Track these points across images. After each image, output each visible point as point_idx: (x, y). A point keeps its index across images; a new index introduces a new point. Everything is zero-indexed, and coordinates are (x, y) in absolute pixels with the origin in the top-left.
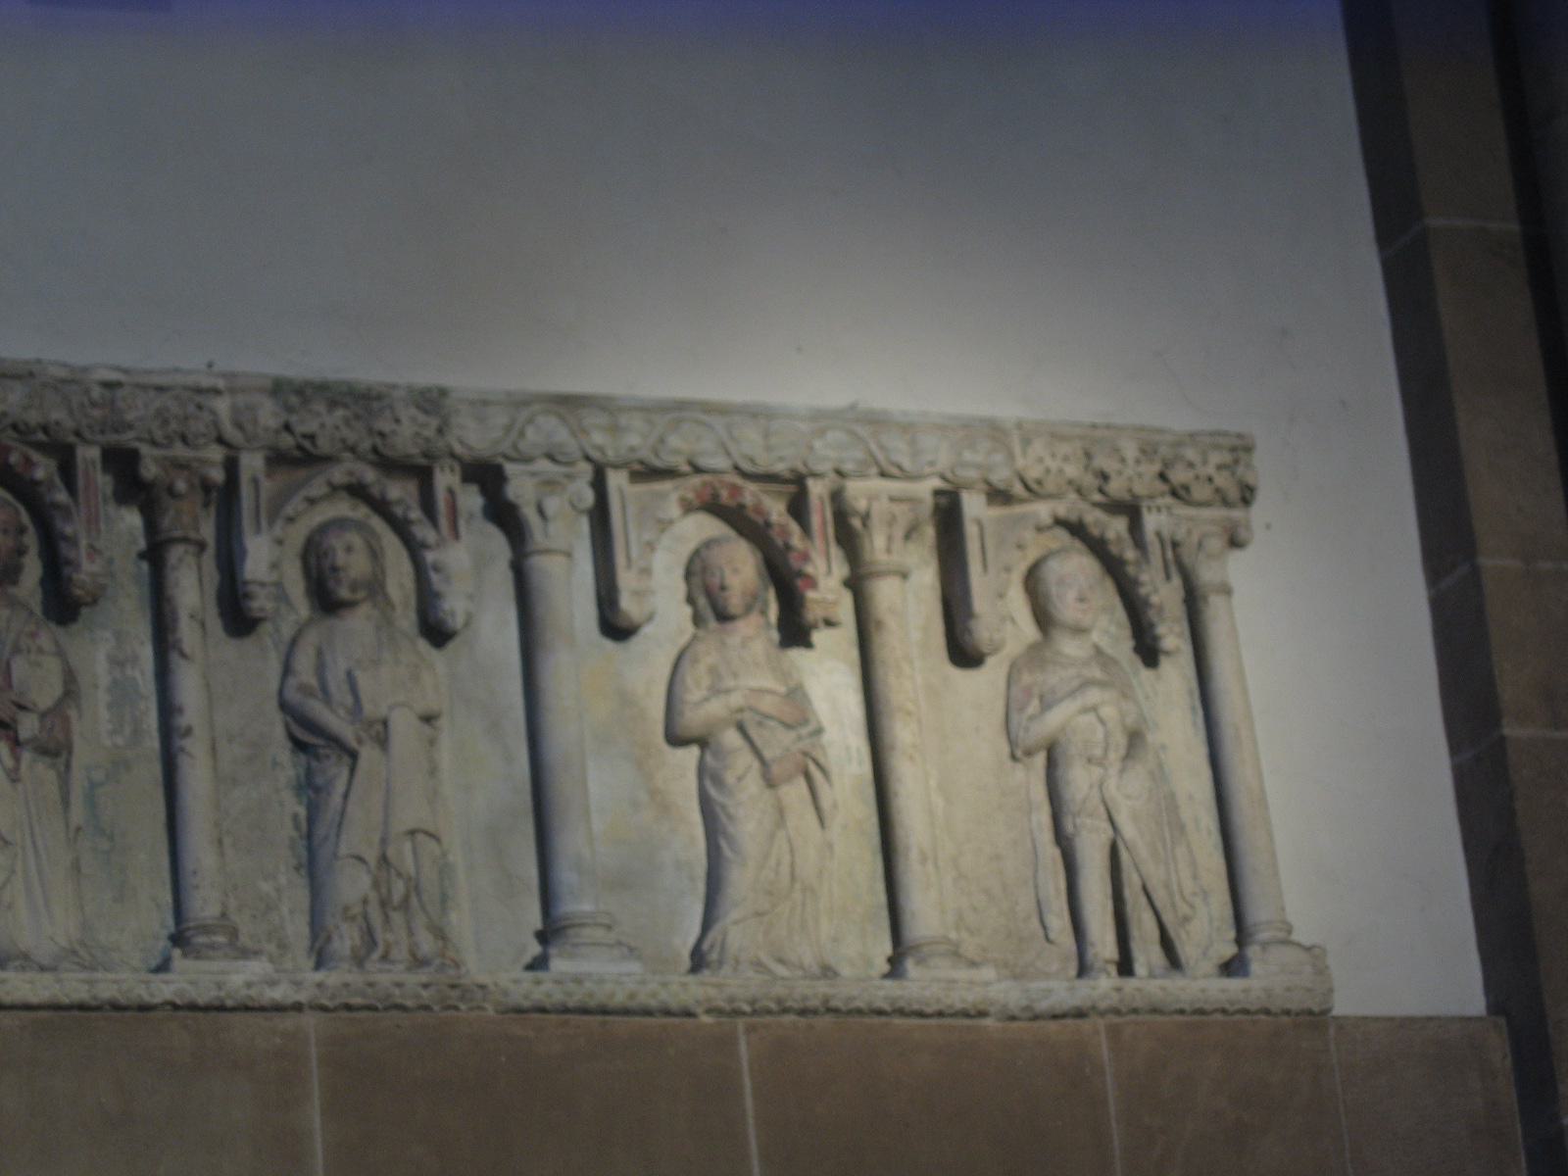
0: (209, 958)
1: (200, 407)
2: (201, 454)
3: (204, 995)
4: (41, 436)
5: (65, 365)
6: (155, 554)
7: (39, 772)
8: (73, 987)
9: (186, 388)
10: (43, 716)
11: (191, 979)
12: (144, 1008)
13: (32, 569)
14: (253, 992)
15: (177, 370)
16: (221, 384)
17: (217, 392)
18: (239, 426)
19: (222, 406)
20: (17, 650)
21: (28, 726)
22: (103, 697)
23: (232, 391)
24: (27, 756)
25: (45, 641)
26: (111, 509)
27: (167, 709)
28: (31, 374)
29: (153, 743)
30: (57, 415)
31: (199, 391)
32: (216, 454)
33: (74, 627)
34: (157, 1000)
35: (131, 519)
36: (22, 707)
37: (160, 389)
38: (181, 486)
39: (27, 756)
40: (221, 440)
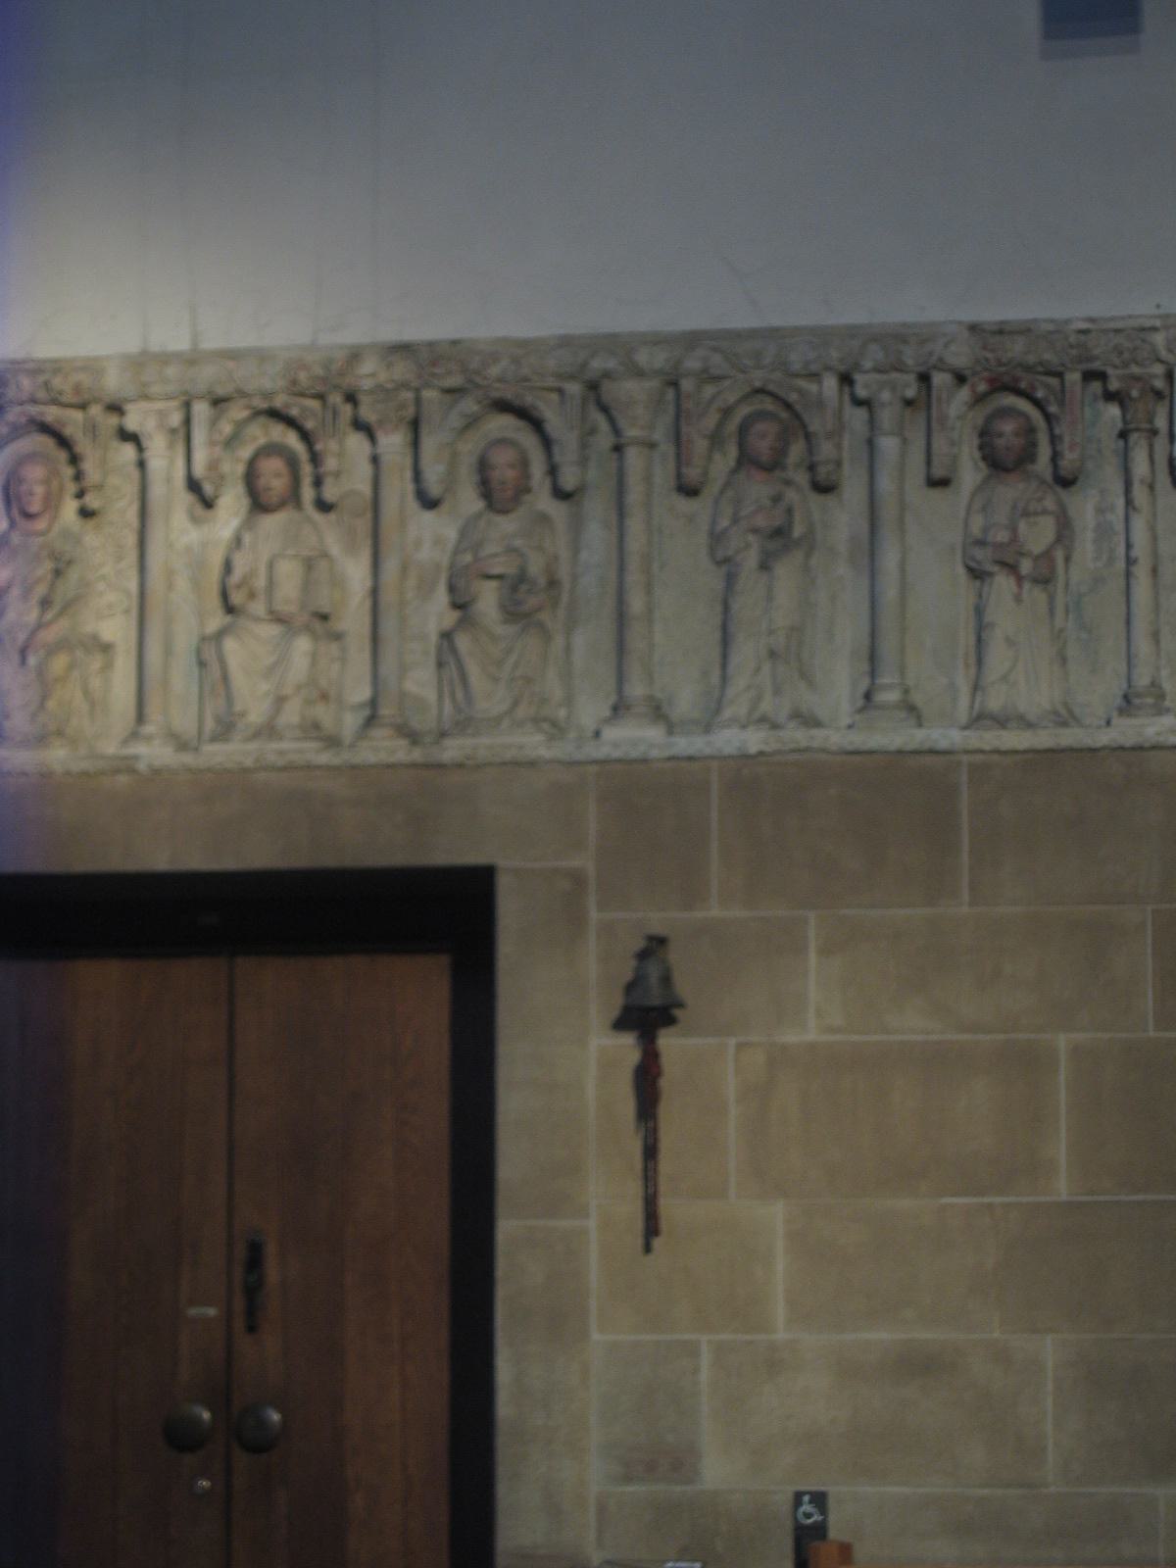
0: (1135, 716)
1: (1143, 341)
2: (1149, 370)
3: (1129, 741)
4: (1040, 369)
5: (1052, 321)
6: (1123, 435)
7: (1036, 596)
8: (1043, 739)
9: (1134, 329)
10: (1036, 559)
11: (1126, 731)
12: (1093, 750)
13: (1044, 452)
14: (1161, 739)
15: (1130, 317)
16: (1158, 323)
17: (1154, 329)
18: (1170, 351)
19: (1159, 339)
20: (1026, 514)
21: (1026, 566)
22: (1090, 535)
23: (1166, 328)
24: (1027, 586)
25: (1049, 503)
26: (1101, 405)
27: (1129, 546)
28: (1029, 330)
29: (1121, 565)
30: (1047, 356)
31: (1143, 329)
32: (1158, 369)
33: (1074, 489)
34: (1099, 745)
35: (1114, 411)
36: (1022, 554)
37: (1117, 331)
38: (1135, 393)
39: (1027, 586)
40: (1162, 362)
